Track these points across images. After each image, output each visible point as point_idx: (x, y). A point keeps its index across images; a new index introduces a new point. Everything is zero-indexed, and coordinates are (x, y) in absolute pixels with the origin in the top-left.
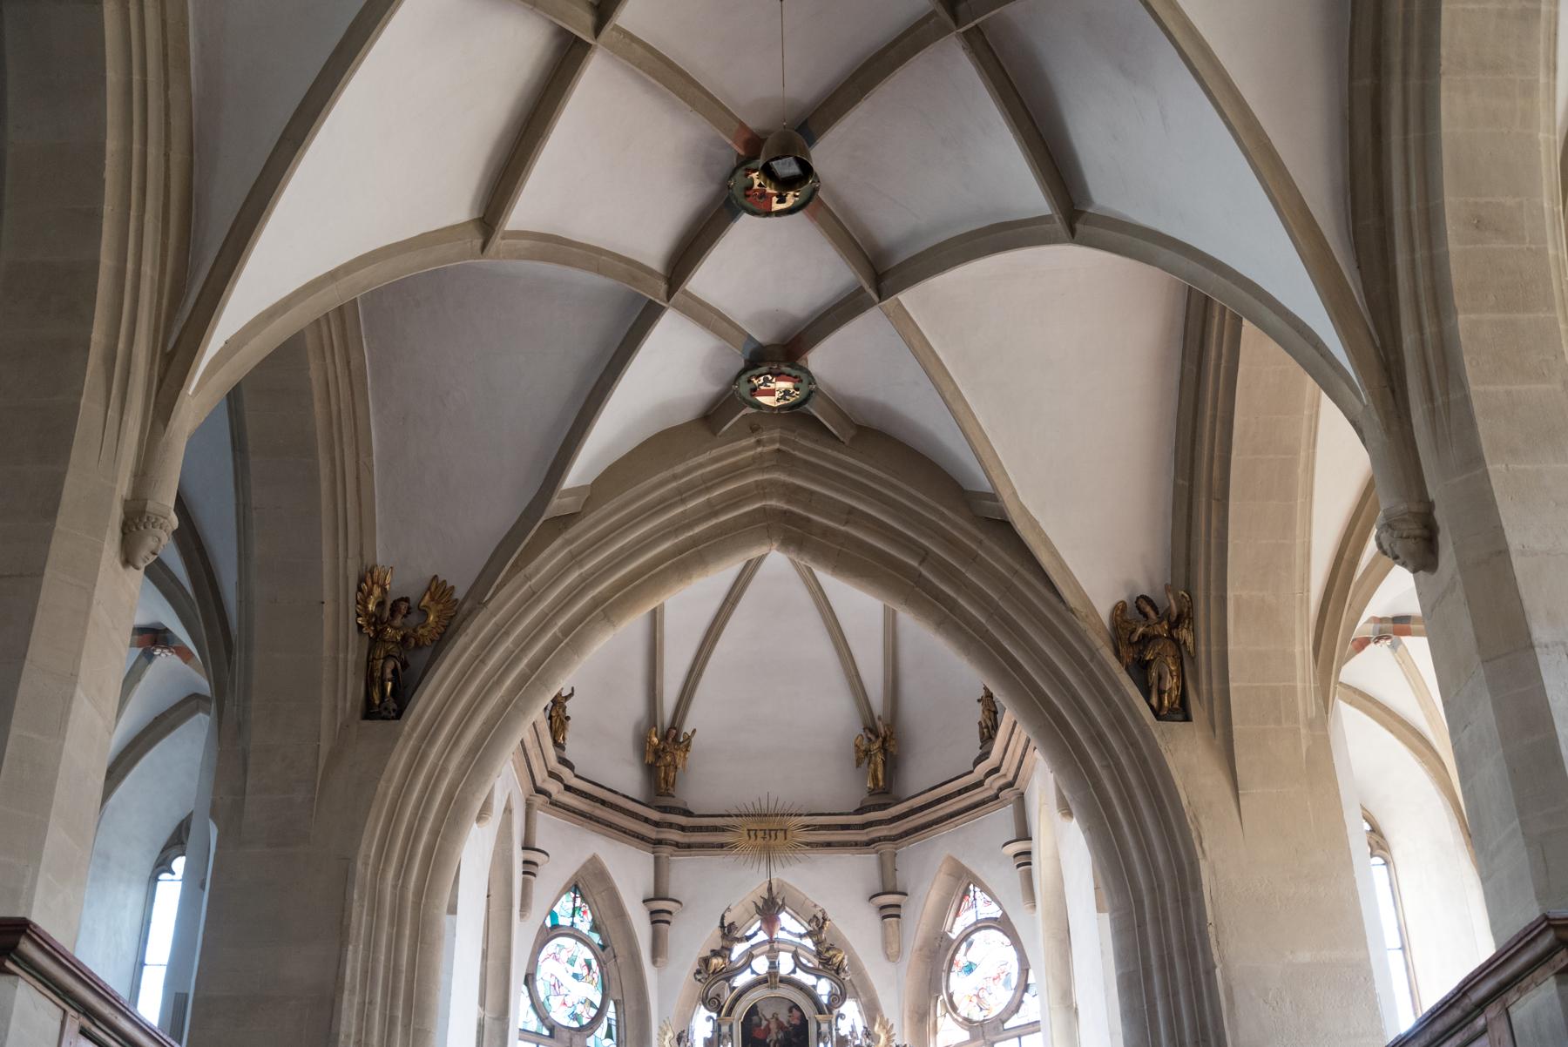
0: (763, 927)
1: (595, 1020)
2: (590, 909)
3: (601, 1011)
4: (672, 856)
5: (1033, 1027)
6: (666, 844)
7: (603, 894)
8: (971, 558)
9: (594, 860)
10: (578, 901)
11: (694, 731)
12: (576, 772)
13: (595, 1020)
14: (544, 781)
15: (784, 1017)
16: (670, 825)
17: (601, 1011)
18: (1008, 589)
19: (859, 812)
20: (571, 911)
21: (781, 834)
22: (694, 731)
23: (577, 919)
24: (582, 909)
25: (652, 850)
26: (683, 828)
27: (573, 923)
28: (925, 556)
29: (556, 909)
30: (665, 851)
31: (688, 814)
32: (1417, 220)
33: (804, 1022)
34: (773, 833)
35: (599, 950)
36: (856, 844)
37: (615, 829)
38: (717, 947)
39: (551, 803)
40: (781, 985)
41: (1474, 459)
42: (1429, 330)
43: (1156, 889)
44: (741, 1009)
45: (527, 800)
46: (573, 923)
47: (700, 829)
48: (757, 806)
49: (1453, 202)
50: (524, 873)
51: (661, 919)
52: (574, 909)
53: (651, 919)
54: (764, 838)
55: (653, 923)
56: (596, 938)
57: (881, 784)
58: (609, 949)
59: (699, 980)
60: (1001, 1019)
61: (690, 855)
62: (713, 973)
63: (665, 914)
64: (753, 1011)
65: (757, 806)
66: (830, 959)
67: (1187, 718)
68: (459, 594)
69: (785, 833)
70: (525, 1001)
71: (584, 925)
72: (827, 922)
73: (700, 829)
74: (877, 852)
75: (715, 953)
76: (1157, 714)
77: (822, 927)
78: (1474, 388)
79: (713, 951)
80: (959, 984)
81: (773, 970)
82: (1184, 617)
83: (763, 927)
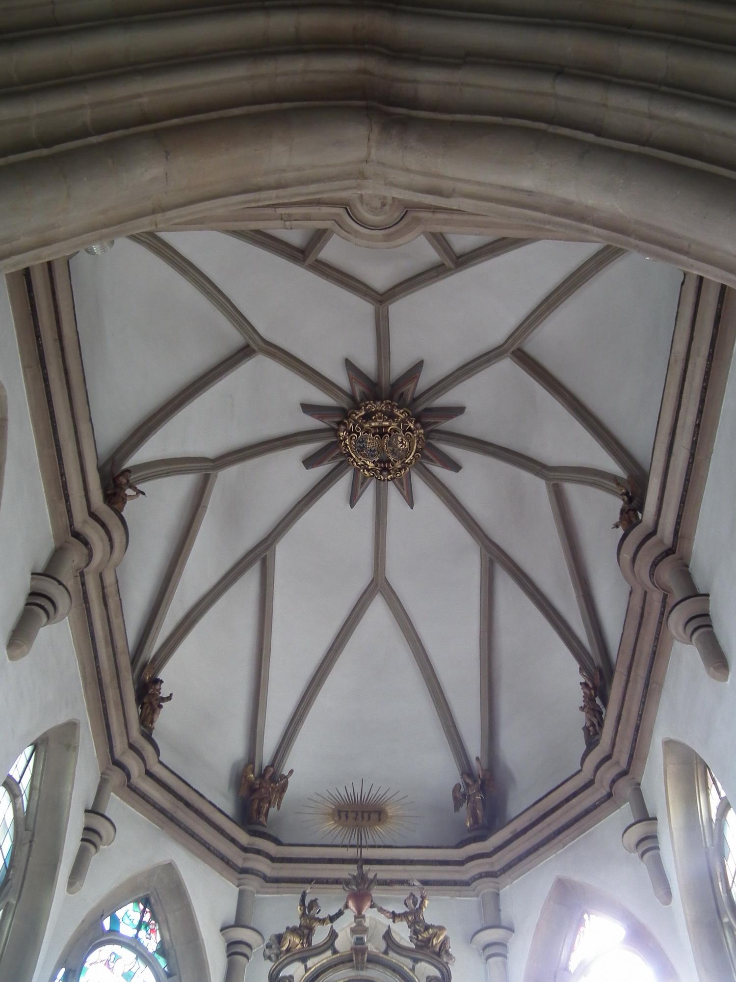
0: (351, 904)
2: (159, 929)
4: (257, 892)
6: (252, 874)
7: (177, 913)
9: (170, 868)
10: (147, 917)
11: (291, 772)
12: (161, 758)
14: (123, 753)
16: (258, 852)
20: (136, 923)
21: (374, 816)
22: (291, 772)
23: (142, 934)
24: (151, 927)
25: (237, 882)
27: (137, 936)
29: (119, 914)
31: (277, 842)
34: (366, 815)
35: (163, 976)
37: (198, 841)
38: (296, 922)
39: (129, 786)
40: (370, 966)
45: (102, 774)
46: (137, 936)
48: (350, 791)
50: (83, 840)
51: (239, 950)
52: (141, 922)
53: (228, 950)
54: (356, 819)
55: (230, 955)
56: (162, 962)
57: (481, 821)
58: (175, 977)
59: (270, 958)
61: (278, 893)
62: (288, 950)
63: (244, 946)
65: (350, 791)
66: (429, 940)
69: (380, 815)
72: (427, 902)
74: (477, 896)
75: (293, 931)
77: (421, 908)
79: (288, 928)
81: (359, 946)
83: (351, 904)
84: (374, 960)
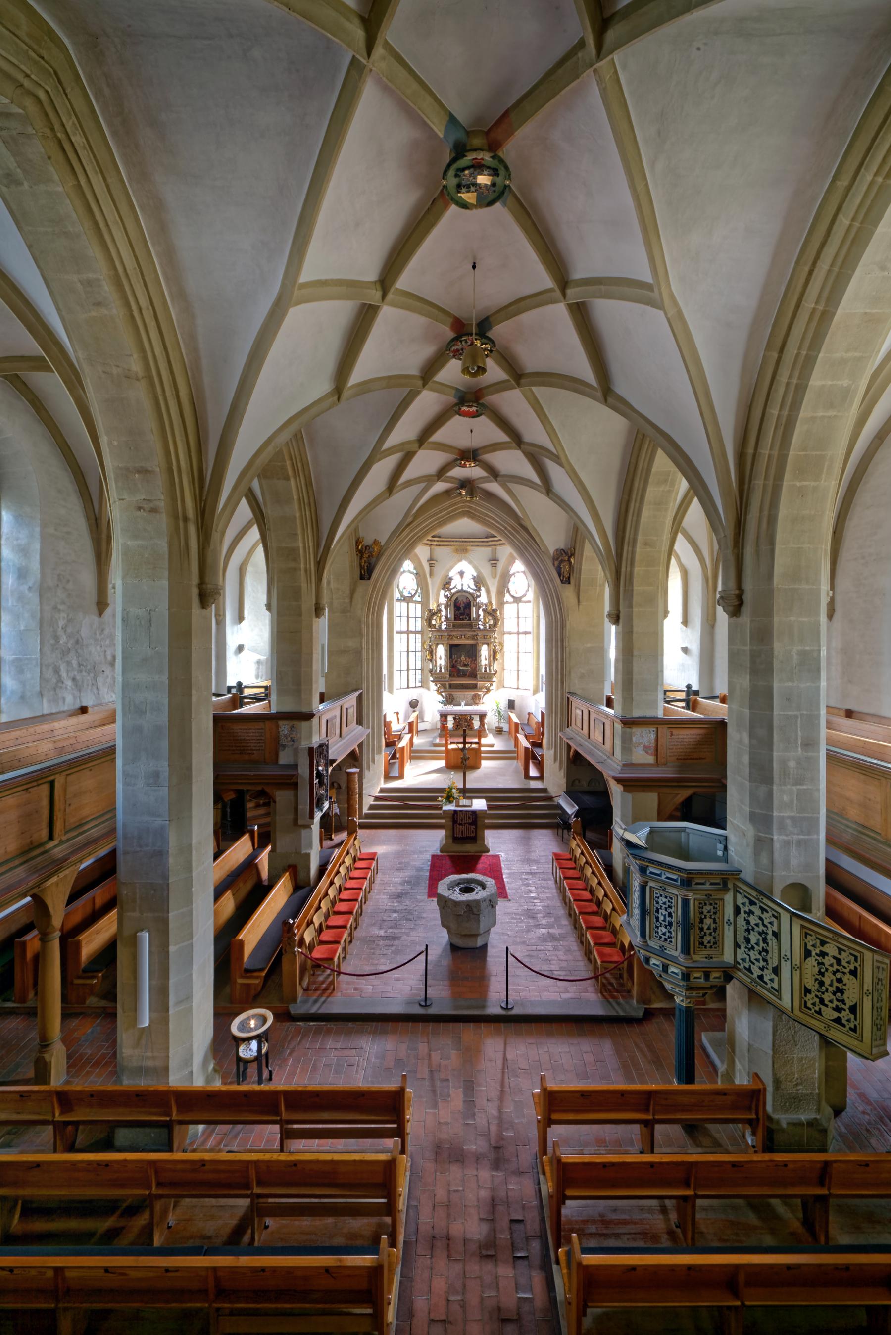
1: (415, 593)
3: (417, 591)
5: (529, 602)
8: (518, 532)
13: (415, 593)
15: (465, 601)
17: (417, 591)
18: (527, 542)
19: (486, 537)
26: (438, 541)
28: (506, 528)
30: (433, 547)
32: (631, 540)
33: (470, 602)
36: (486, 546)
41: (631, 606)
42: (628, 569)
43: (557, 622)
44: (454, 599)
47: (443, 541)
49: (640, 538)
60: (521, 598)
64: (457, 599)
67: (569, 583)
68: (382, 544)
70: (397, 592)
71: (412, 569)
73: (443, 541)
76: (562, 582)
78: (635, 588)
80: (511, 586)
82: (573, 555)
84: (465, 591)
